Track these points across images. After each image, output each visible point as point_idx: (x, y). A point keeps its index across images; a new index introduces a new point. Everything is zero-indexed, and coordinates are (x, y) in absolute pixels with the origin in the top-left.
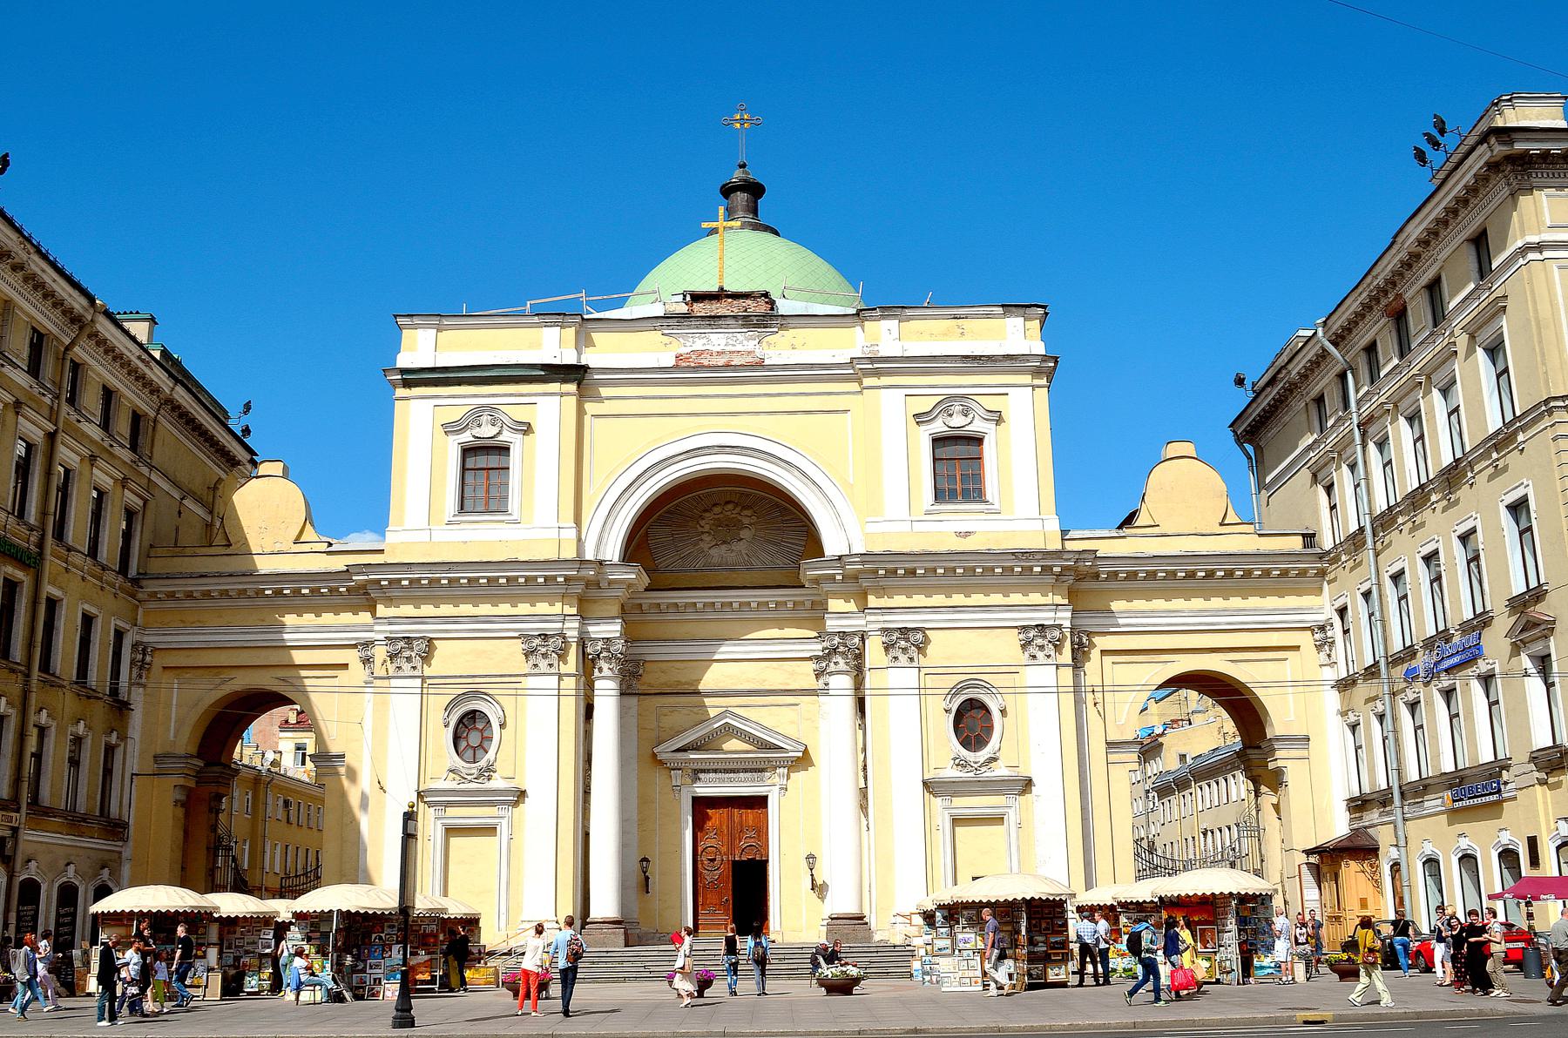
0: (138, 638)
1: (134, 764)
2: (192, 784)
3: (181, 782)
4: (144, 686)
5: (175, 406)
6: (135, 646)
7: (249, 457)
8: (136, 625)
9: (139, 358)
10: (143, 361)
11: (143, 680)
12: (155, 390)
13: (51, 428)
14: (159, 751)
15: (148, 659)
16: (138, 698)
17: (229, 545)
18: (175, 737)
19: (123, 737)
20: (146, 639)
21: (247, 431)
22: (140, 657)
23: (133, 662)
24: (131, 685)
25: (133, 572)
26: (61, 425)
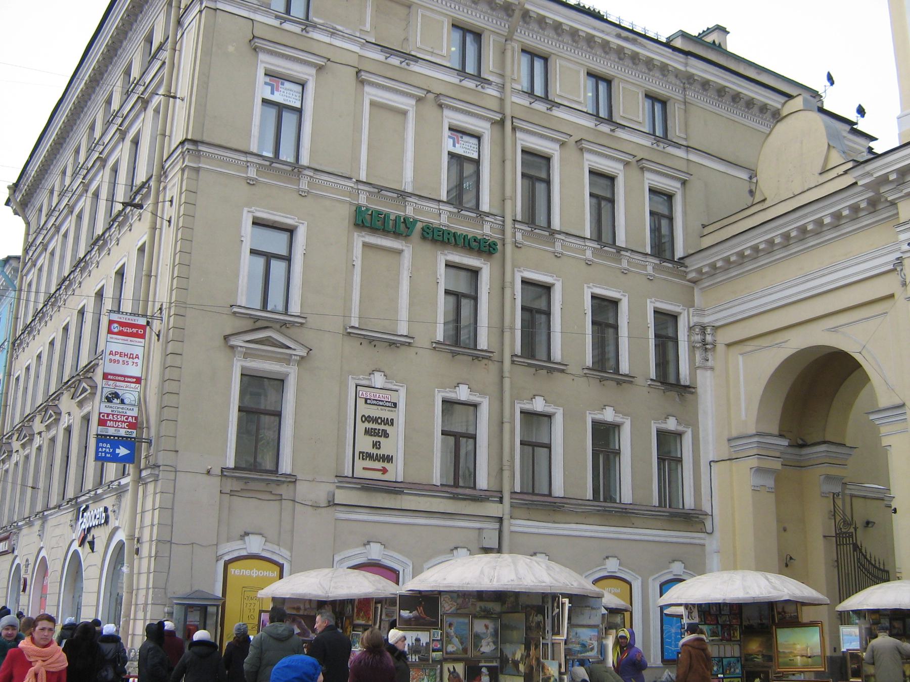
0: (694, 320)
1: (709, 451)
2: (777, 465)
3: (754, 462)
4: (712, 369)
5: (705, 85)
6: (691, 329)
7: (848, 128)
8: (693, 306)
9: (619, 36)
10: (626, 39)
11: (709, 364)
12: (664, 69)
13: (498, 117)
14: (734, 434)
15: (709, 338)
16: (706, 384)
17: (764, 200)
18: (746, 416)
19: (694, 424)
20: (706, 320)
21: (861, 111)
22: (698, 338)
23: (692, 348)
24: (693, 369)
25: (679, 253)
26: (508, 112)
